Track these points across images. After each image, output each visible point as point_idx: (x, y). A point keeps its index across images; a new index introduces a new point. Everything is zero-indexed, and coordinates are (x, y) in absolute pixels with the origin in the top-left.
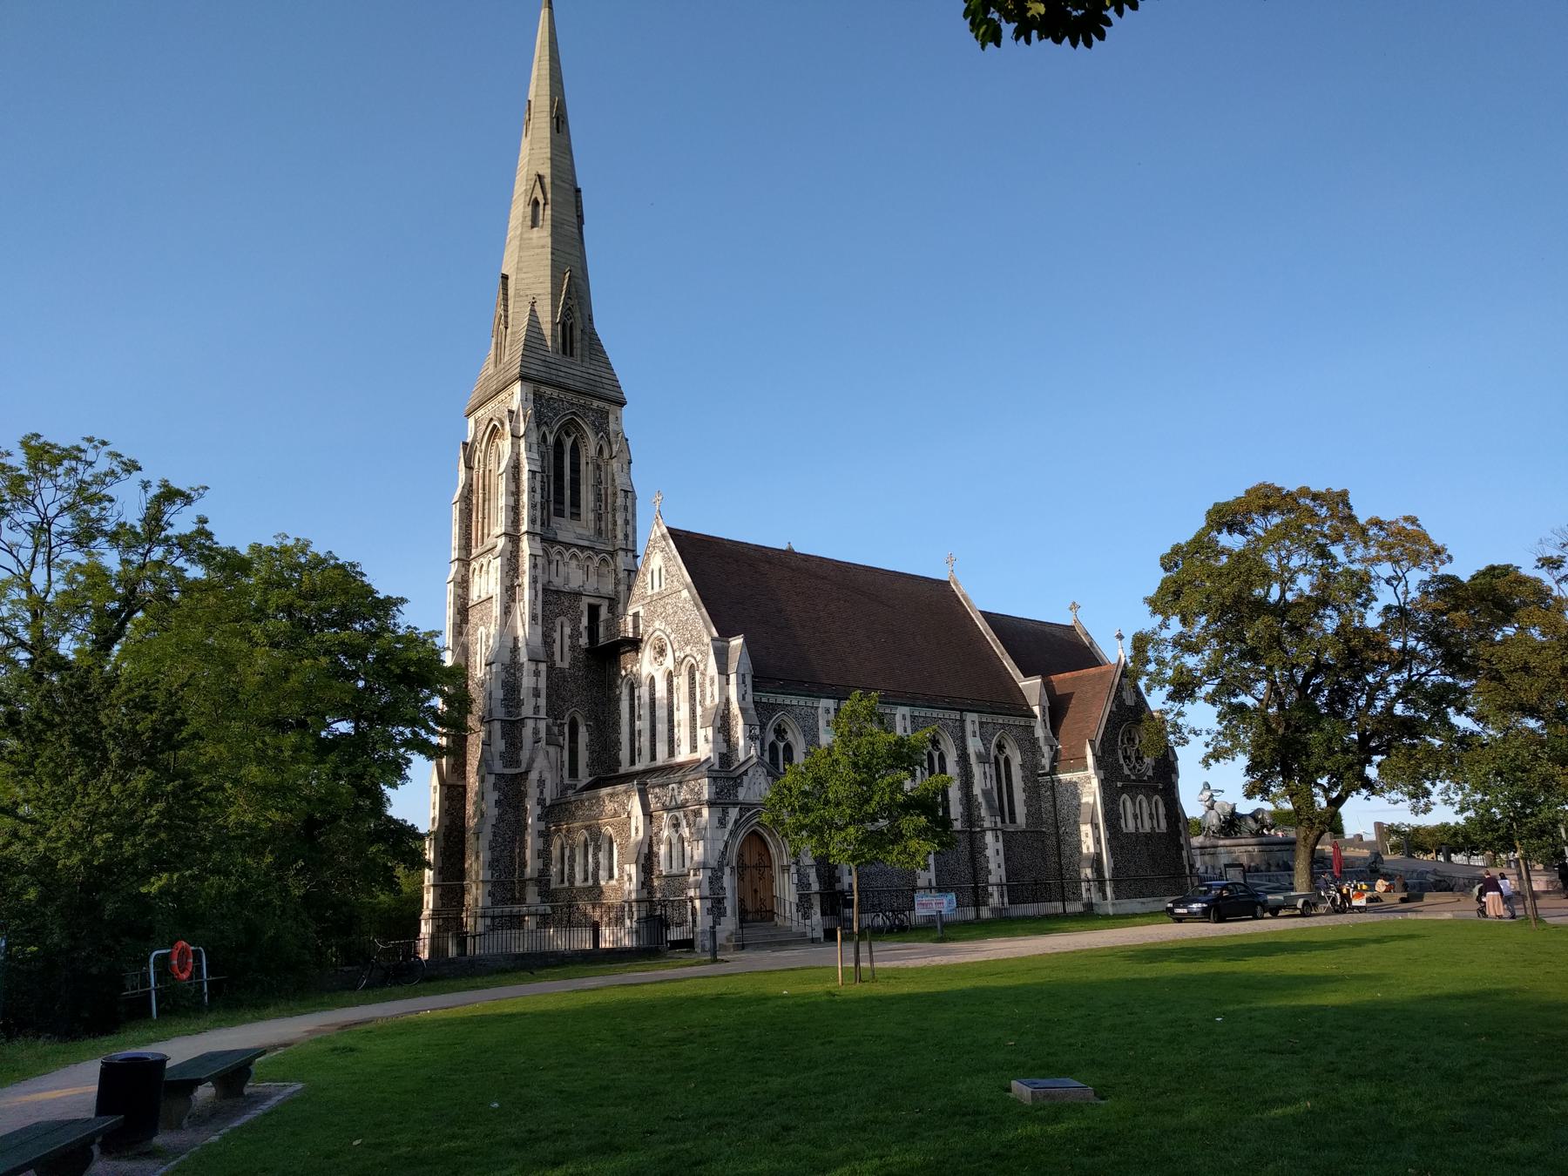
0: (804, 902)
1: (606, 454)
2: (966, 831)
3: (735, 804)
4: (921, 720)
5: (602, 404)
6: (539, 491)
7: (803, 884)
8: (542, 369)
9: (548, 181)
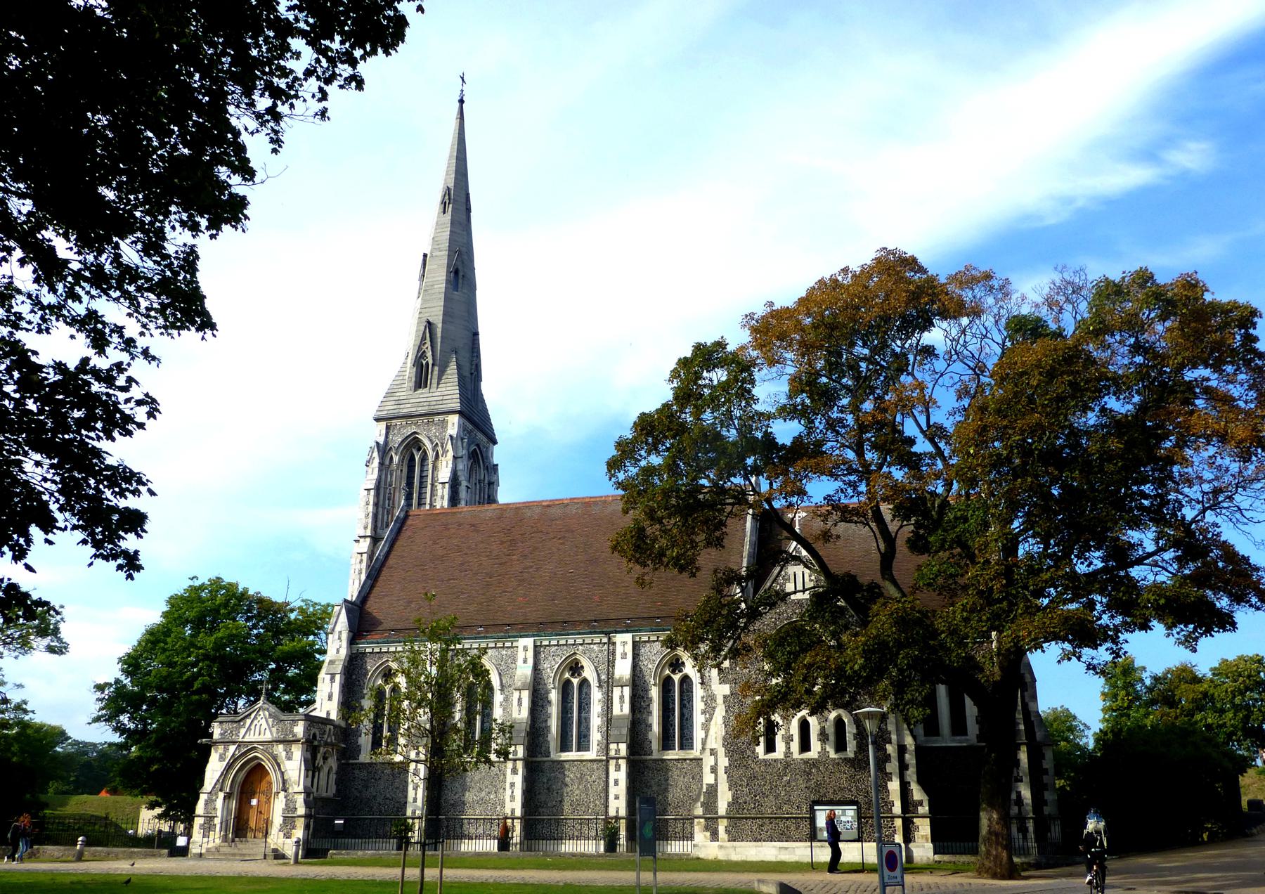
0: (289, 821)
2: (601, 761)
3: (234, 742)
4: (553, 649)
5: (441, 418)
6: (371, 503)
7: (290, 807)
8: (395, 407)
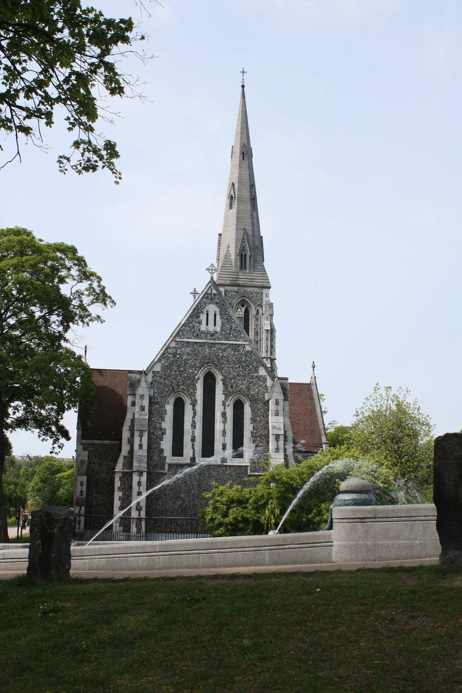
1: (260, 314)
9: (236, 186)
